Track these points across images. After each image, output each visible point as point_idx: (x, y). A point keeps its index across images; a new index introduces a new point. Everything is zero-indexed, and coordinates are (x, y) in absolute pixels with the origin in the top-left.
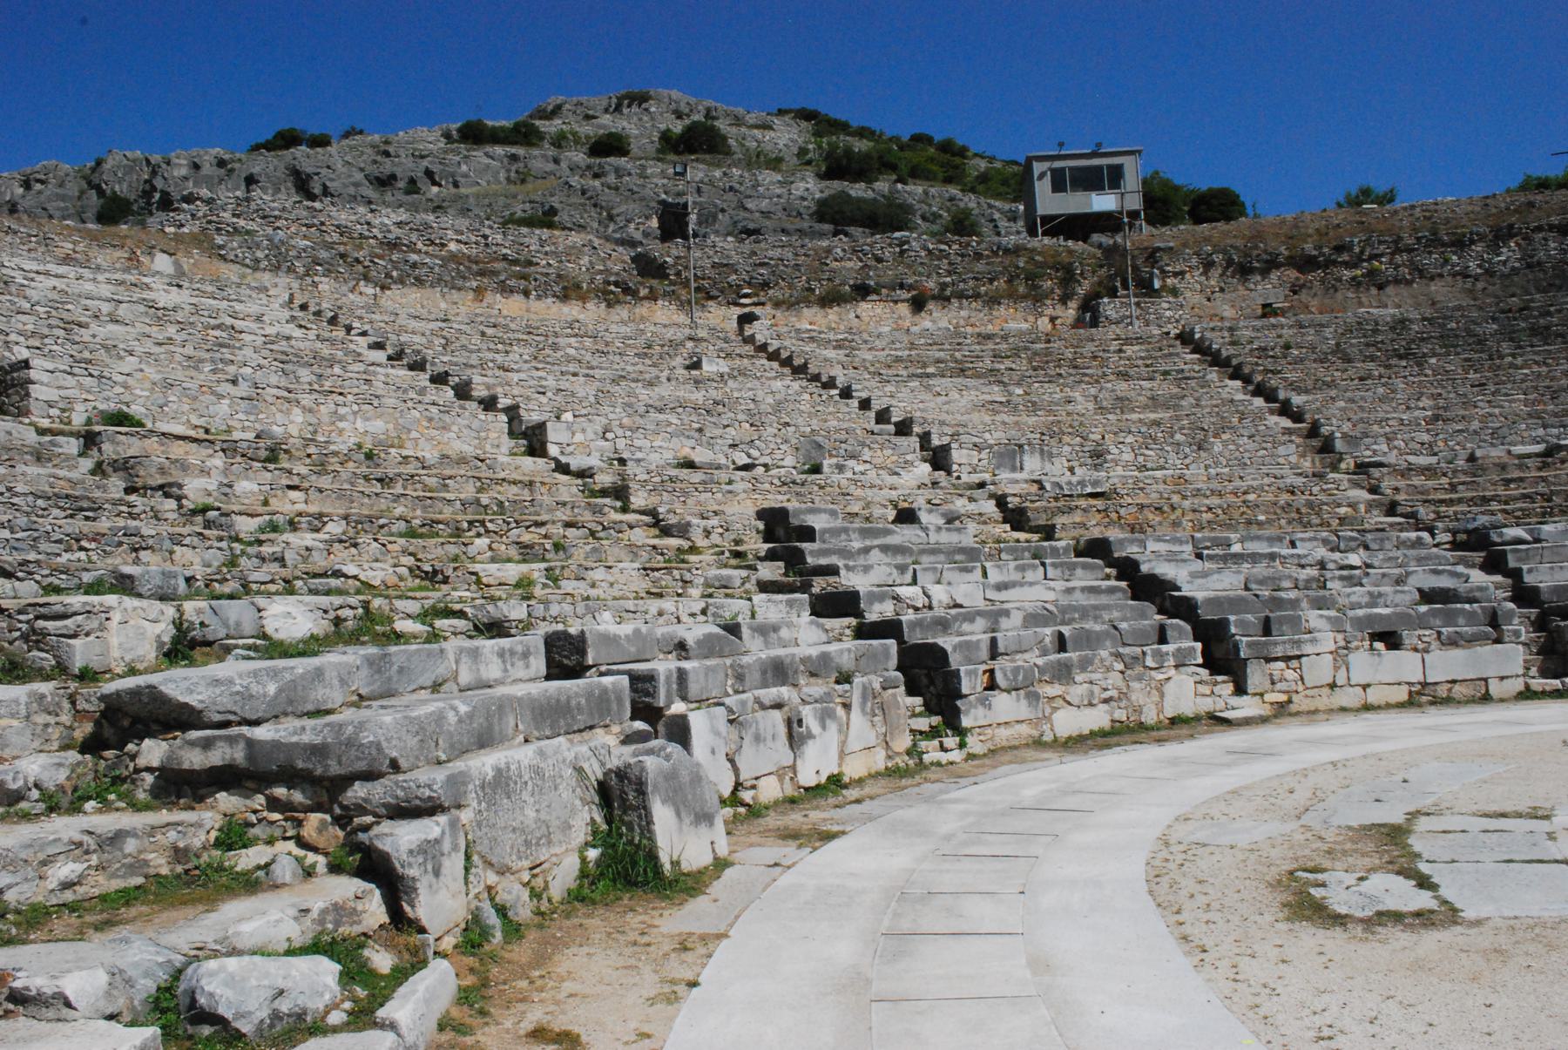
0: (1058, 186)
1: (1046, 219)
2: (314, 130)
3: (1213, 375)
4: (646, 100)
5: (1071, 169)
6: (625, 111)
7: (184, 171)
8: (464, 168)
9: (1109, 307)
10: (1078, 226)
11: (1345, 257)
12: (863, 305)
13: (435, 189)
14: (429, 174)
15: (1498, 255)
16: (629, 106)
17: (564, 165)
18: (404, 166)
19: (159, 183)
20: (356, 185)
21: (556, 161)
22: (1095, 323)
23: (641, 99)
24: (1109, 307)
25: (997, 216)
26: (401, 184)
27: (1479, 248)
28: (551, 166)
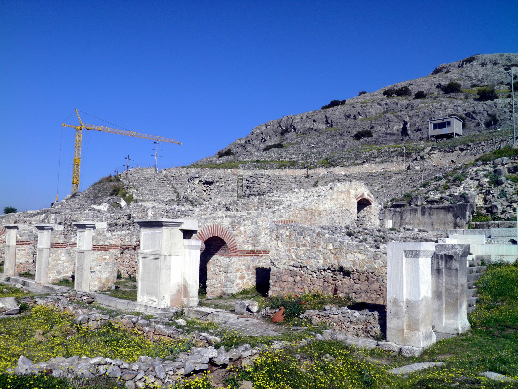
0: (435, 128)
2: (341, 100)
4: (472, 61)
5: (439, 124)
6: (464, 66)
7: (299, 120)
8: (371, 110)
11: (469, 148)
12: (364, 165)
13: (361, 117)
14: (359, 113)
16: (466, 64)
17: (399, 105)
18: (353, 112)
19: (293, 124)
20: (340, 118)
21: (397, 104)
23: (470, 60)
26: (352, 117)
28: (396, 106)
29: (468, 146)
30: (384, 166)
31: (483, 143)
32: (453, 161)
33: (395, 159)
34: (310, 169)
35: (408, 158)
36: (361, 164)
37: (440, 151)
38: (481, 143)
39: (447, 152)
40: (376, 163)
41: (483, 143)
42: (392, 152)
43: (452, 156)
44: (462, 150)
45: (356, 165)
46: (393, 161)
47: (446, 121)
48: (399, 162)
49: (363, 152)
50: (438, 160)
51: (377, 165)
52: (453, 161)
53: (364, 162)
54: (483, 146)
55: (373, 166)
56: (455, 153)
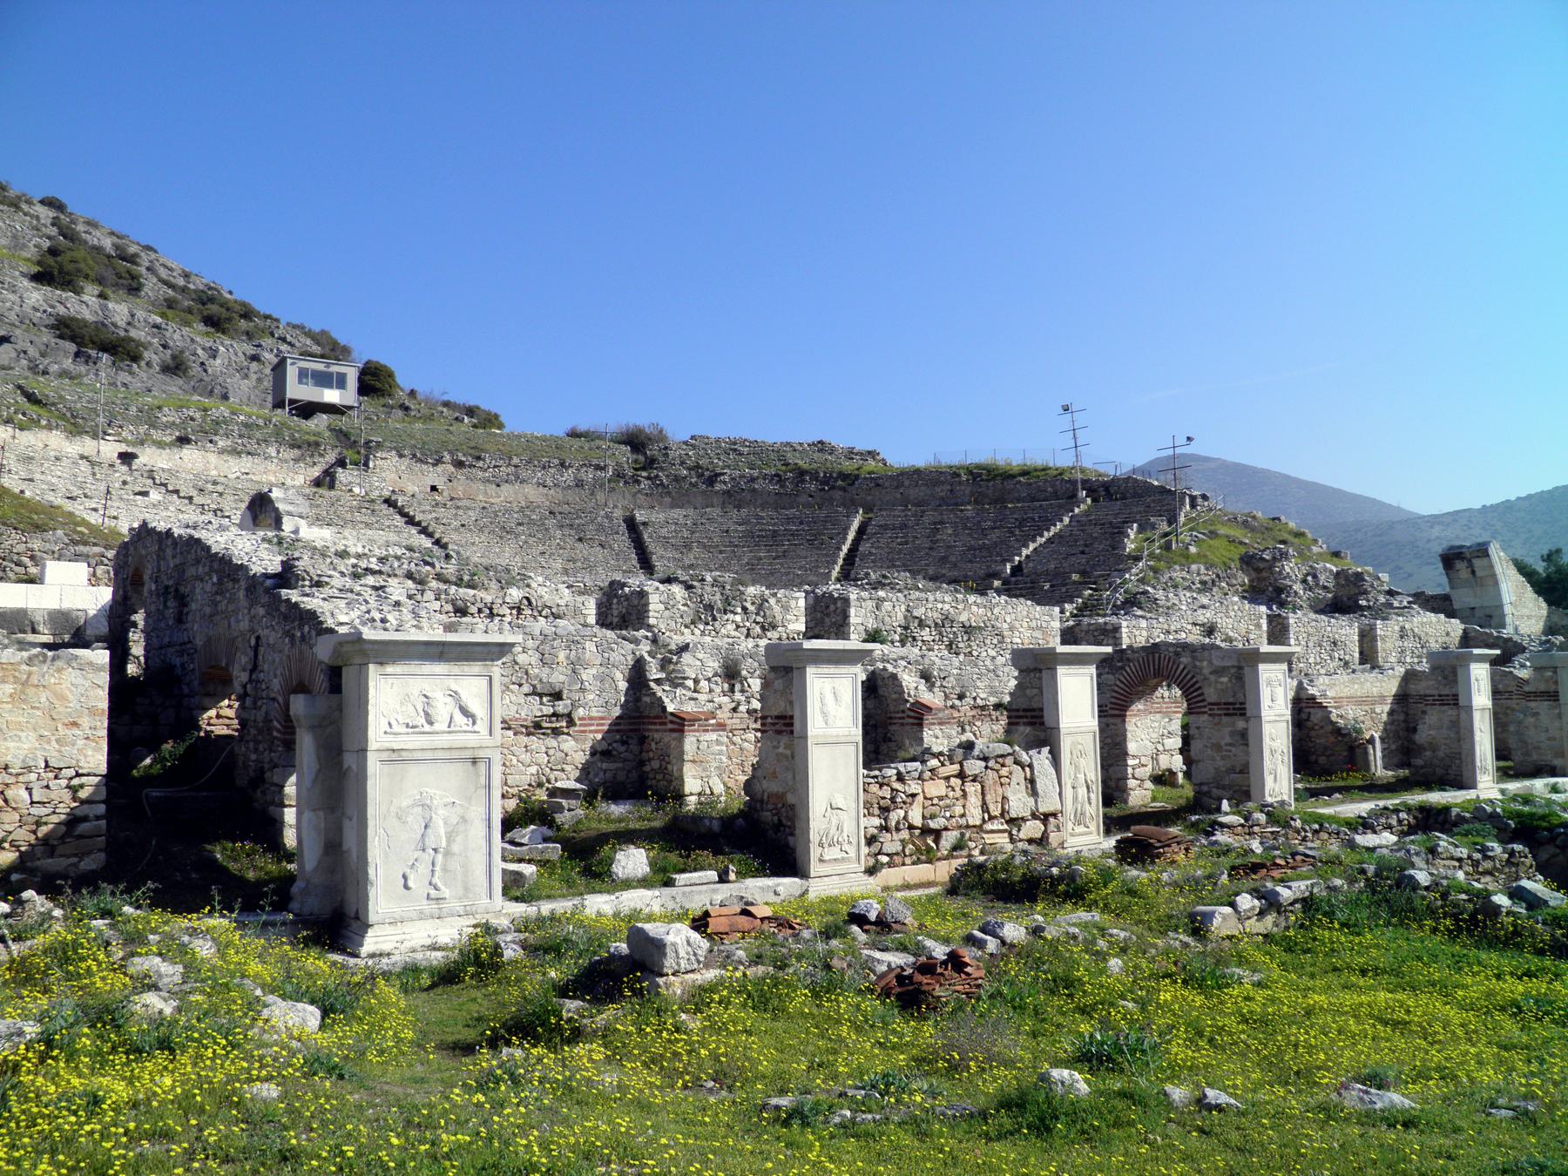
1: (292, 402)
3: (414, 531)
9: (342, 475)
10: (307, 410)
11: (481, 464)
22: (332, 487)
24: (342, 475)
25: (200, 352)
29: (479, 458)
30: (246, 463)
31: (515, 460)
32: (434, 488)
33: (272, 451)
34: (21, 429)
35: (312, 456)
36: (170, 445)
37: (401, 456)
38: (510, 458)
39: (421, 461)
40: (222, 452)
41: (515, 460)
42: (246, 425)
43: (435, 476)
44: (459, 464)
45: (160, 445)
46: (268, 458)
47: (335, 369)
48: (286, 461)
49: (160, 408)
50: (394, 476)
51: (225, 457)
52: (434, 488)
53: (183, 441)
55: (213, 458)
56: (440, 468)
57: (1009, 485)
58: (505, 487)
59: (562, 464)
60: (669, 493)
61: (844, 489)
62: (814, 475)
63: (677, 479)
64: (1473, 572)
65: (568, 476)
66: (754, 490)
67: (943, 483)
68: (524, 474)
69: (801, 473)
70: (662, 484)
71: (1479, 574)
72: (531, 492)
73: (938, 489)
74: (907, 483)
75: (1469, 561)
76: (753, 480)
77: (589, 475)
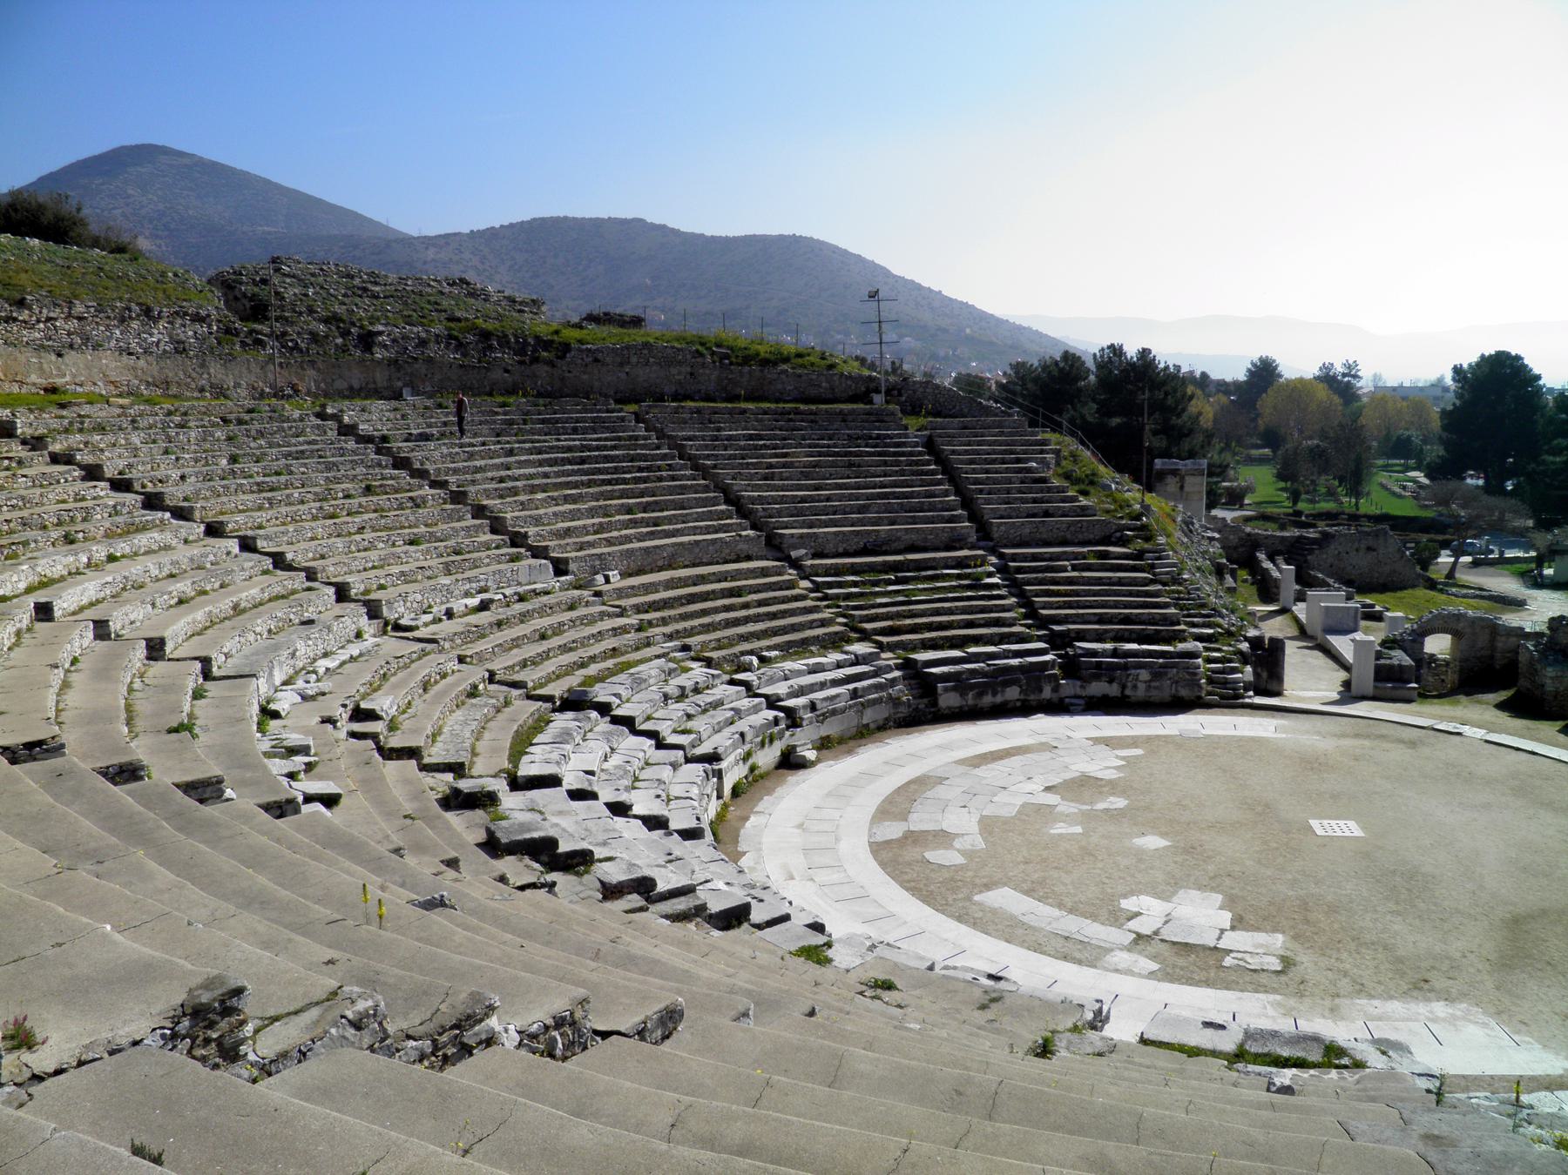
15: (151, 335)
27: (135, 325)
29: (21, 303)
31: (79, 308)
41: (79, 308)
54: (80, 319)
57: (771, 373)
58: (71, 357)
59: (147, 311)
60: (312, 363)
61: (552, 364)
62: (504, 341)
63: (314, 338)
64: (1182, 487)
65: (158, 334)
66: (430, 360)
67: (680, 363)
68: (97, 333)
69: (485, 335)
70: (296, 347)
71: (1187, 489)
72: (109, 362)
73: (674, 371)
74: (634, 359)
75: (1182, 479)
76: (423, 343)
77: (189, 333)
